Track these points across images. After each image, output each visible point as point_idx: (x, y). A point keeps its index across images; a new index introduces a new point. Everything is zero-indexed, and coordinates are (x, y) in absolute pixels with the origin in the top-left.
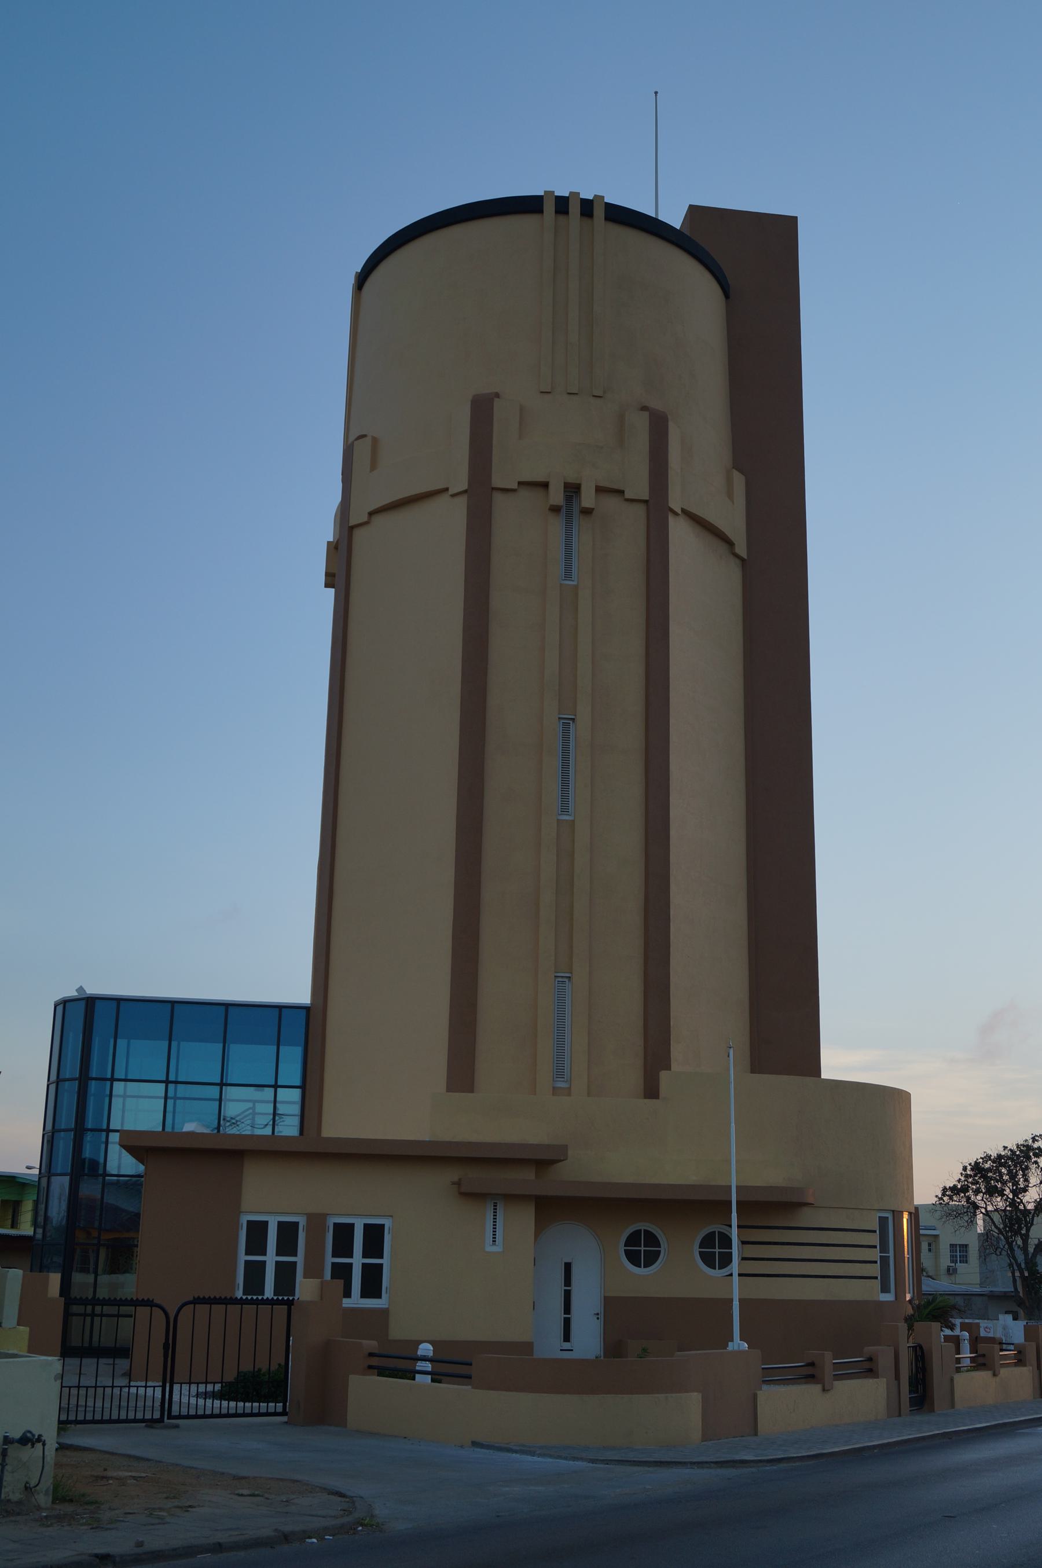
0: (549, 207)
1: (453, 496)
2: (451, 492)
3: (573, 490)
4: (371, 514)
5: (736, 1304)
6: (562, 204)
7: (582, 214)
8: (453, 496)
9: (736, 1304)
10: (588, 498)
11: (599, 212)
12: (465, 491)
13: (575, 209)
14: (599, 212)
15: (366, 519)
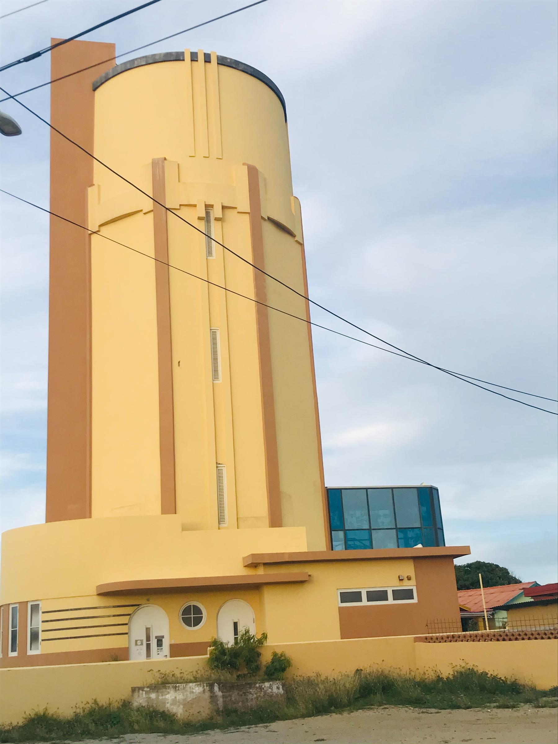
0: (188, 57)
1: (145, 214)
2: (144, 211)
3: (208, 207)
4: (101, 226)
5: (482, 587)
6: (194, 57)
7: (205, 61)
8: (145, 214)
9: (482, 587)
10: (217, 212)
11: (214, 60)
12: (152, 211)
13: (201, 58)
14: (214, 60)
15: (97, 230)
